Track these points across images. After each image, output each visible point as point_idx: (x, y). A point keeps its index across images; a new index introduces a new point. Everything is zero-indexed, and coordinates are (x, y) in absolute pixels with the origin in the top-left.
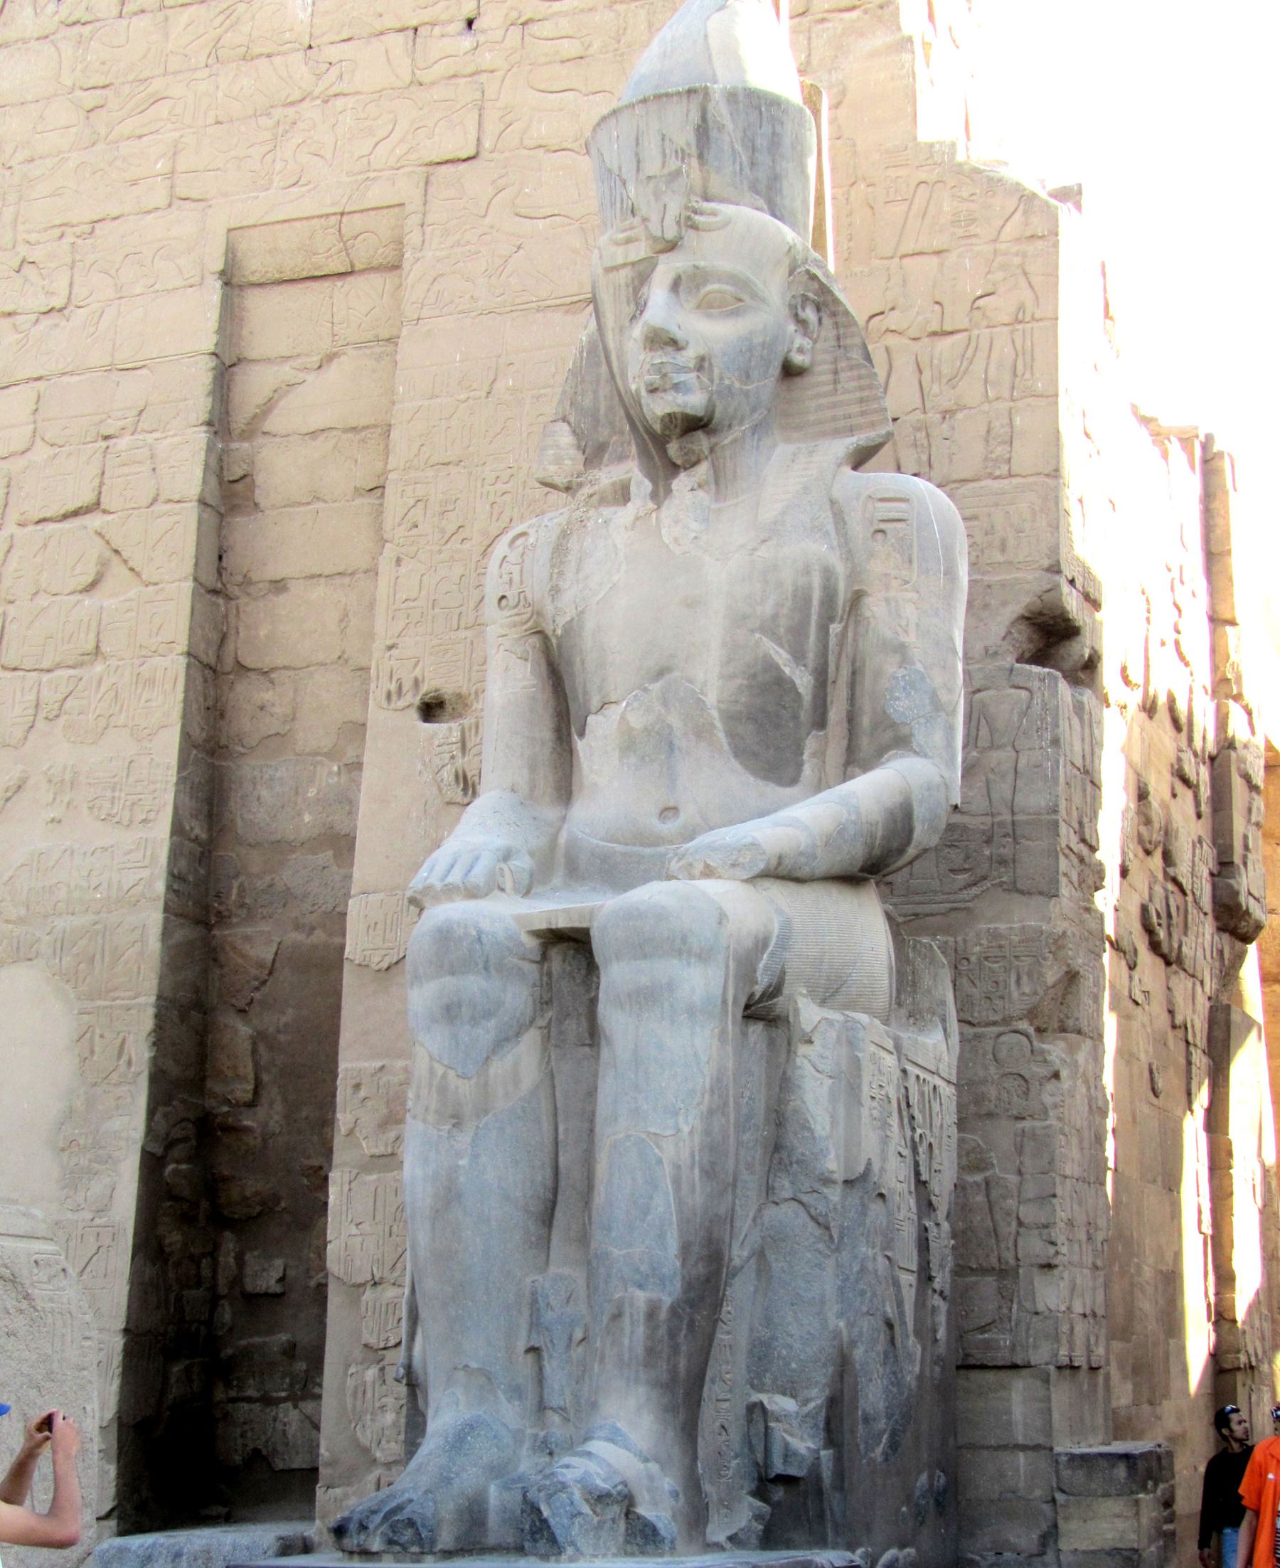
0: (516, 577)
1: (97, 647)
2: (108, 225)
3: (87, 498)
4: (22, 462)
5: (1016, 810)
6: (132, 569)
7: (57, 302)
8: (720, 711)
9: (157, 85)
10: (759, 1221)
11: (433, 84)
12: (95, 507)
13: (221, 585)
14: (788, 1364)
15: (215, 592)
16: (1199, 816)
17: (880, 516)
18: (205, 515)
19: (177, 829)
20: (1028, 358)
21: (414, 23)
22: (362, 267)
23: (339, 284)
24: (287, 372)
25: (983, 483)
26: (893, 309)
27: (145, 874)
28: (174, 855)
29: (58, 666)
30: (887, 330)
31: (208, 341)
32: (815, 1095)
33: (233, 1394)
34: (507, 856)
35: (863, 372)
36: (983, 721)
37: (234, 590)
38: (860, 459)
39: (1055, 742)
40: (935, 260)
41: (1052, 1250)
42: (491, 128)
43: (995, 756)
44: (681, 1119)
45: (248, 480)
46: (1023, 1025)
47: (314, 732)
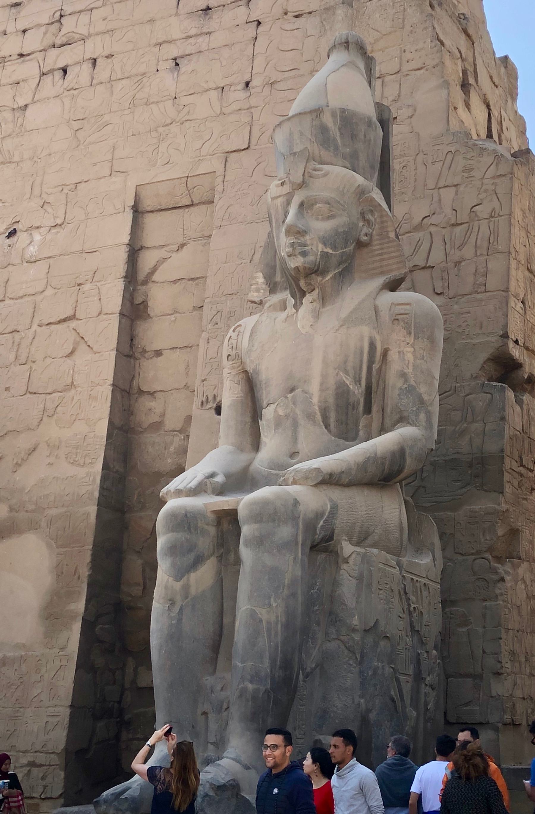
0: (234, 346)
1: (72, 383)
2: (83, 185)
3: (69, 313)
4: (41, 297)
6: (89, 346)
7: (59, 221)
8: (320, 407)
9: (107, 118)
11: (230, 114)
13: (130, 351)
15: (129, 356)
17: (397, 312)
18: (123, 320)
19: (105, 466)
20: (496, 234)
21: (222, 85)
22: (197, 202)
23: (187, 210)
25: (472, 296)
26: (434, 214)
27: (90, 488)
28: (104, 478)
29: (54, 392)
30: (431, 224)
31: (126, 239)
32: (347, 588)
33: (130, 736)
34: (212, 475)
35: (395, 243)
37: (137, 355)
38: (393, 286)
39: (503, 419)
40: (454, 189)
42: (256, 133)
44: (272, 599)
45: (145, 303)
46: (487, 555)
47: (173, 421)
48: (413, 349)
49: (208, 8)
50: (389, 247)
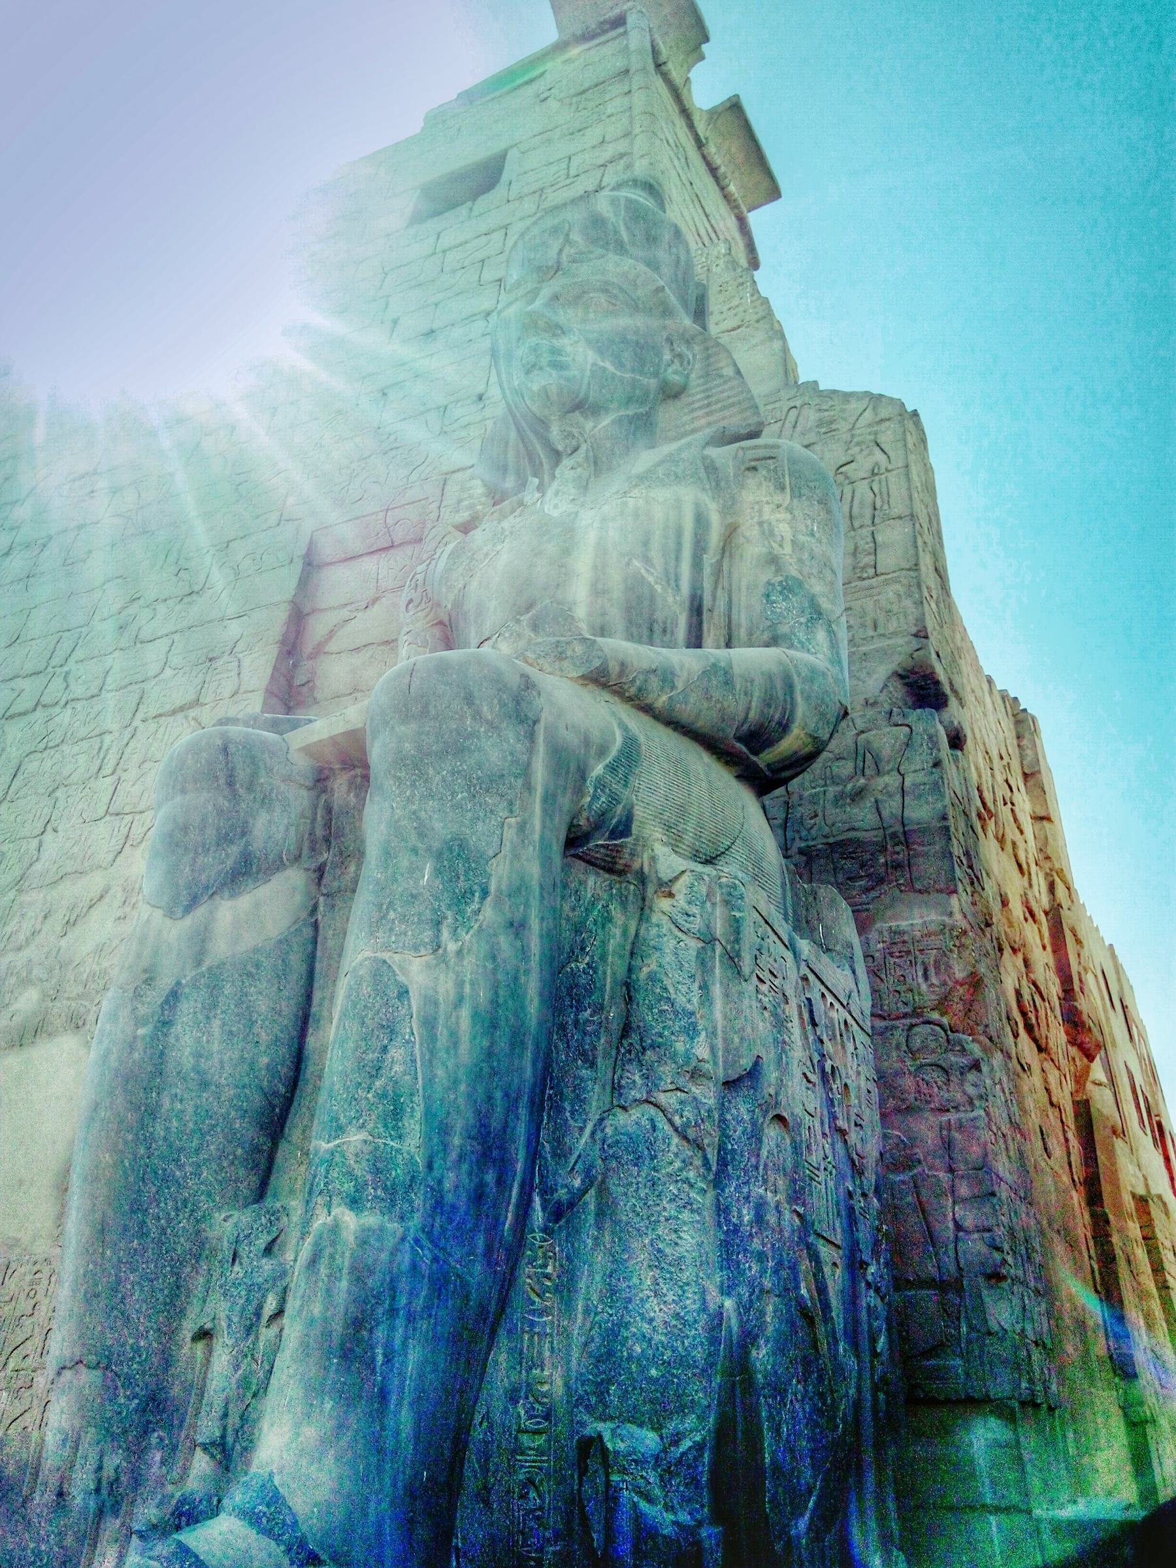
3: (190, 697)
5: (906, 822)
10: (599, 1135)
12: (197, 703)
14: (643, 1369)
16: (1044, 948)
24: (345, 613)
36: (868, 754)
41: (997, 1256)
43: (881, 782)
45: (311, 684)
48: (788, 516)
49: (433, 331)
50: (722, 392)
